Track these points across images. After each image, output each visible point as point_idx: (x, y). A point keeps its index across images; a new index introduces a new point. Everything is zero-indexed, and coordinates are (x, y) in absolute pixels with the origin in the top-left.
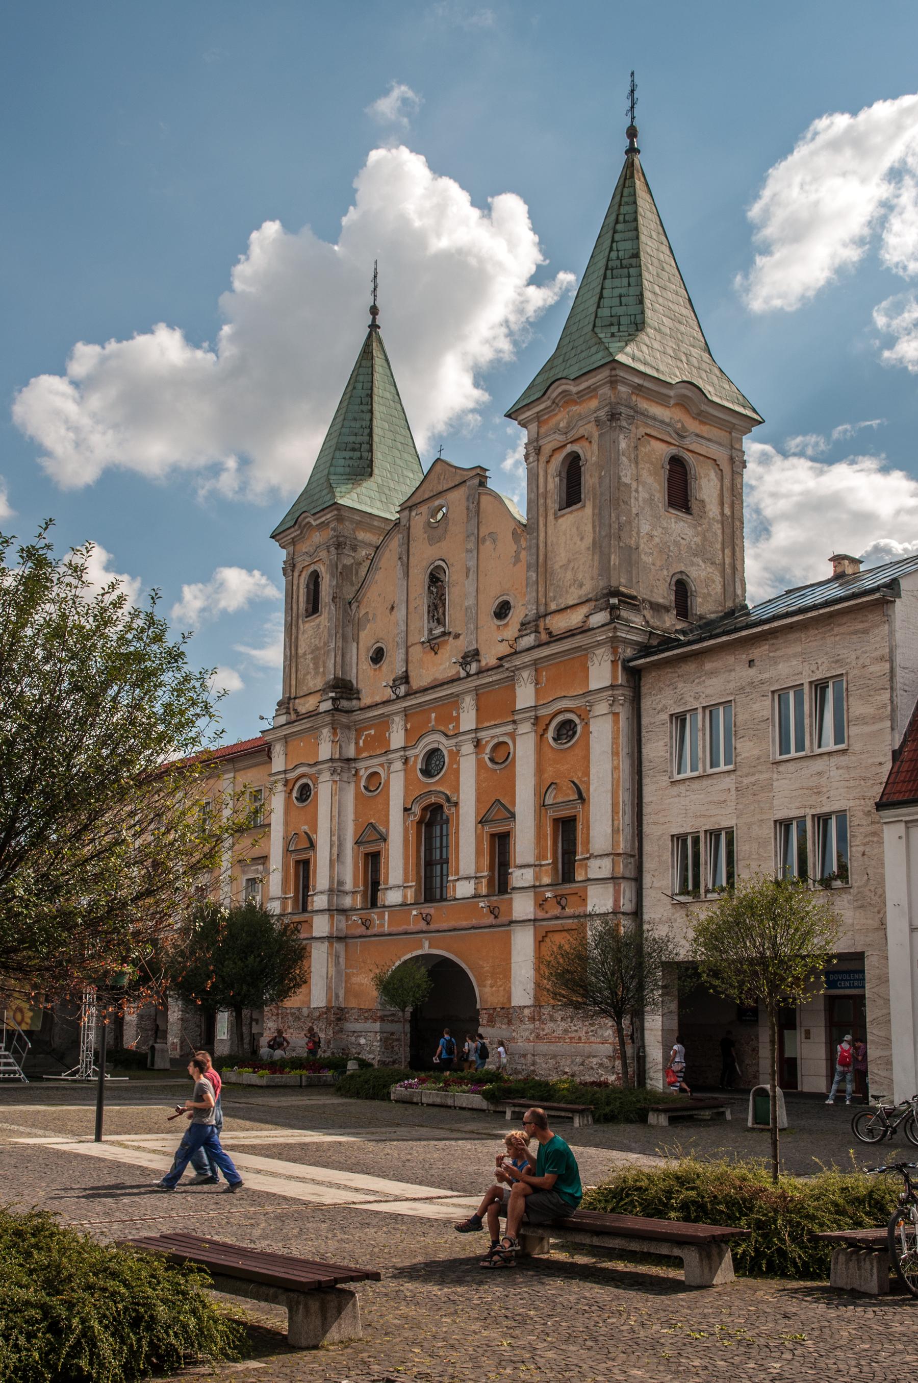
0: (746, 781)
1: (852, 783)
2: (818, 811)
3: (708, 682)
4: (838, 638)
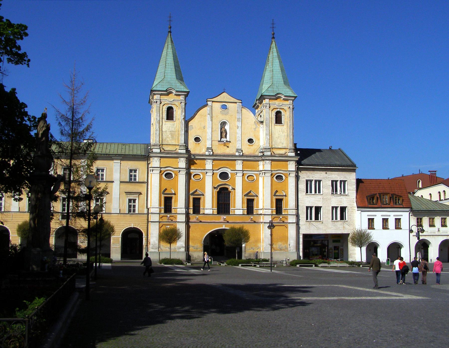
0: (325, 197)
1: (348, 201)
3: (315, 175)
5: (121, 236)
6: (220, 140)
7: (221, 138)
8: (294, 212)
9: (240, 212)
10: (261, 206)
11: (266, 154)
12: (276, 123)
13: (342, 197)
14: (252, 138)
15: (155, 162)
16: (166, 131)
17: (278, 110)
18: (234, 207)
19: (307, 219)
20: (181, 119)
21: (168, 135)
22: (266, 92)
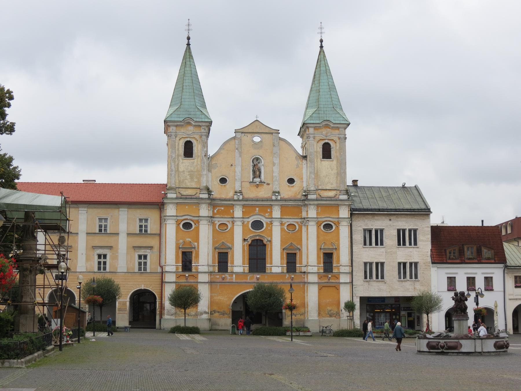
0: (389, 250)
2: (411, 261)
4: (416, 219)
5: (128, 300)
6: (251, 180)
7: (254, 178)
8: (348, 269)
9: (278, 270)
10: (304, 263)
11: (310, 197)
12: (323, 158)
13: (411, 250)
14: (292, 177)
15: (170, 210)
16: (184, 171)
17: (327, 141)
18: (271, 263)
19: (366, 278)
20: (202, 156)
21: (186, 176)
22: (309, 119)
